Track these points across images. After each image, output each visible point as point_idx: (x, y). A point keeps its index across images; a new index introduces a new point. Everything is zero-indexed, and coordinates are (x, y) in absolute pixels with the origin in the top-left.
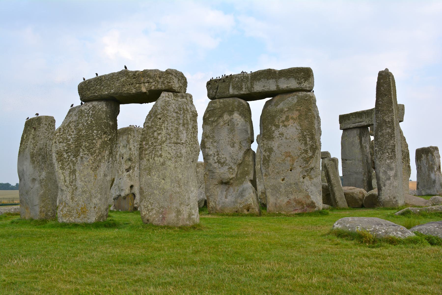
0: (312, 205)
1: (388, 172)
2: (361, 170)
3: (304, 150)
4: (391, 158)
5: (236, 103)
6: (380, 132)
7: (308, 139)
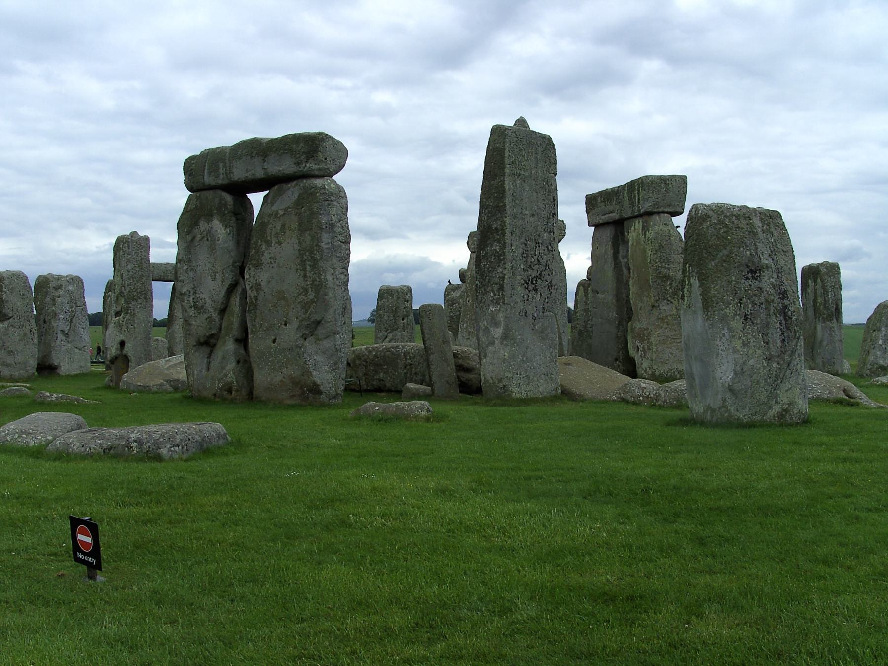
0: (315, 390)
1: (492, 329)
2: (614, 314)
3: (303, 288)
4: (497, 302)
5: (217, 201)
6: (483, 249)
7: (308, 268)
